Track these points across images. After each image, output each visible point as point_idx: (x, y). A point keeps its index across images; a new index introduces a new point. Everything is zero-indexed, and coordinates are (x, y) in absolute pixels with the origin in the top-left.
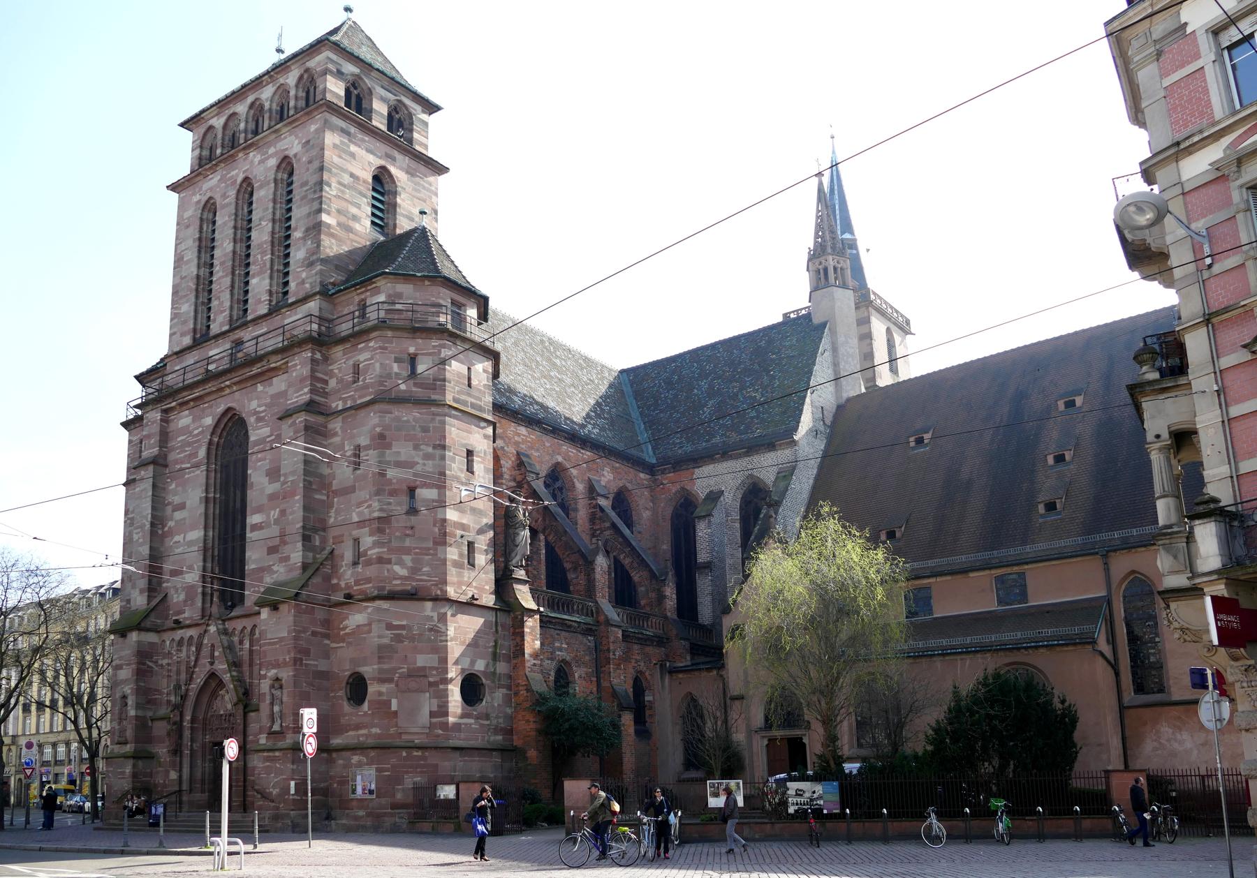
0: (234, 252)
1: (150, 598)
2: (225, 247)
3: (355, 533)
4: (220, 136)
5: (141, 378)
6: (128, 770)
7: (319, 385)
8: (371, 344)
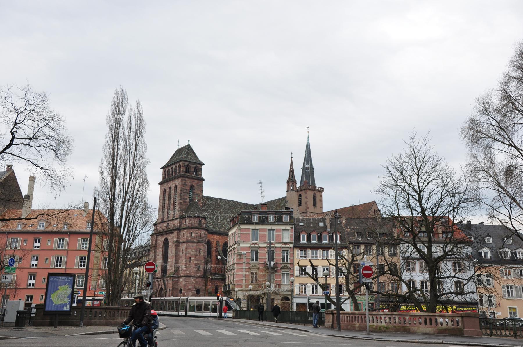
2: (167, 202)
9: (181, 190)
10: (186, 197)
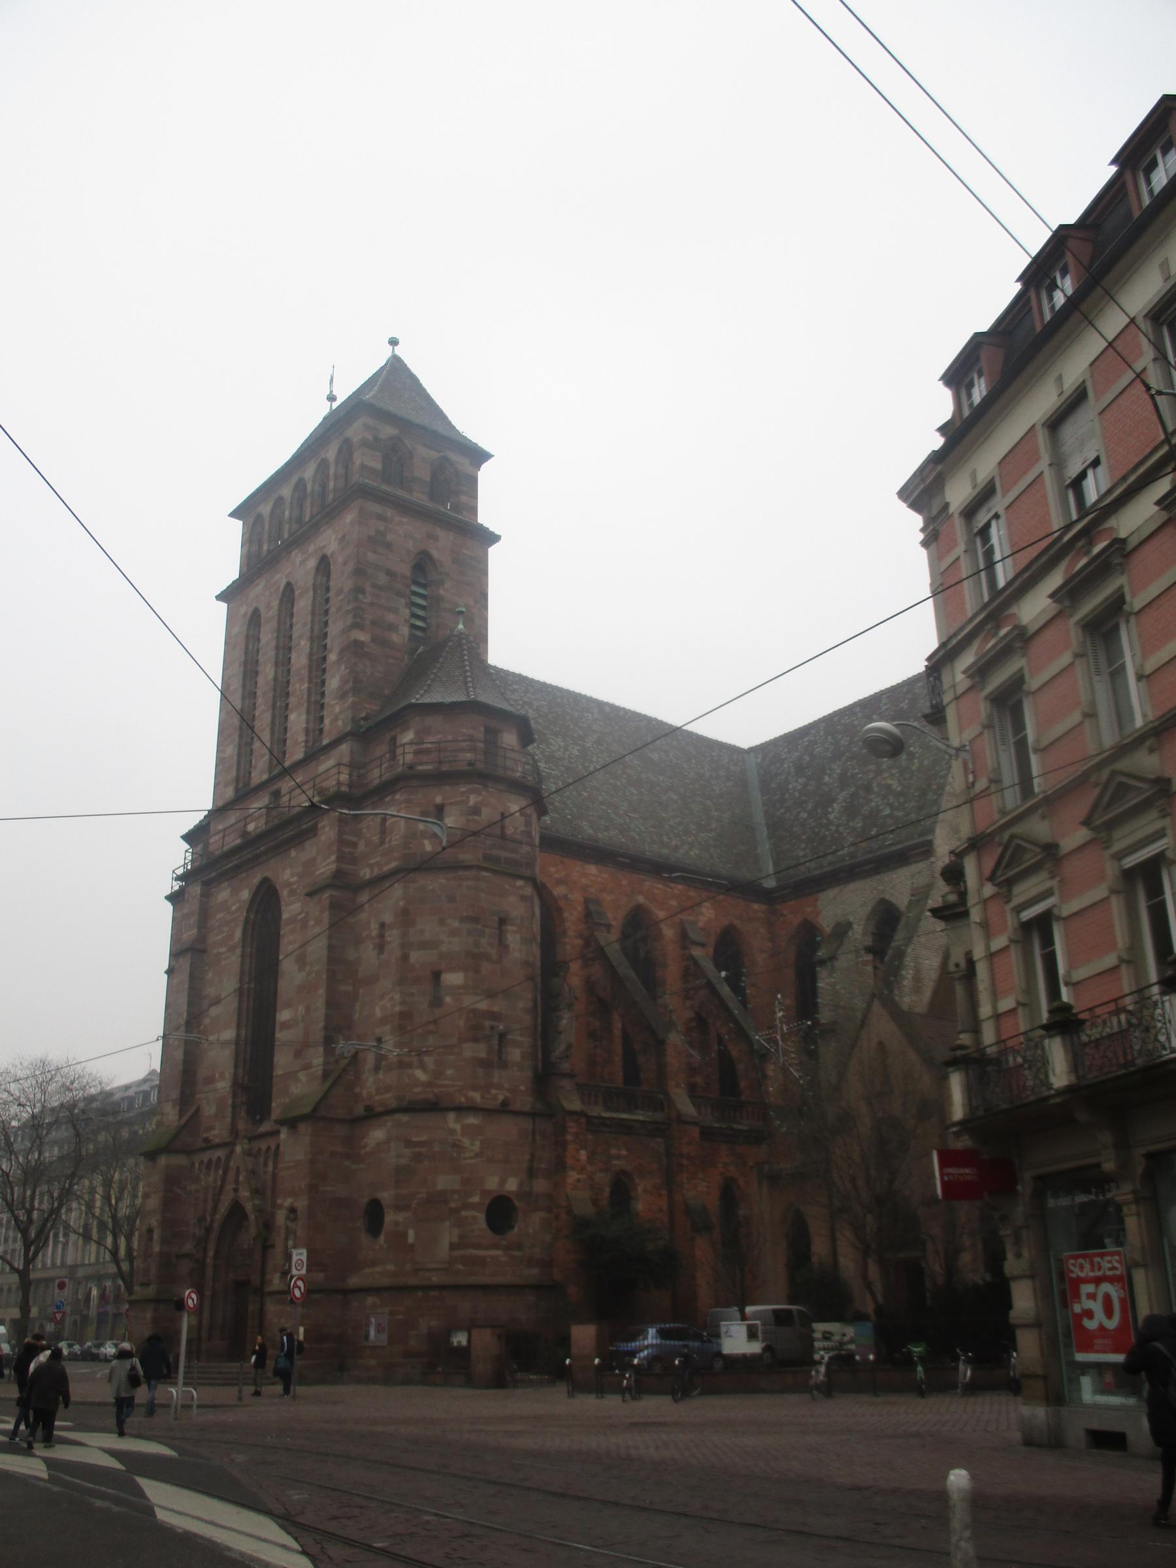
0: (275, 679)
1: (181, 1113)
2: (267, 672)
3: (378, 1031)
4: (267, 527)
5: (189, 838)
6: (149, 1315)
7: (347, 850)
8: (398, 796)
9: (359, 572)
10: (391, 617)
